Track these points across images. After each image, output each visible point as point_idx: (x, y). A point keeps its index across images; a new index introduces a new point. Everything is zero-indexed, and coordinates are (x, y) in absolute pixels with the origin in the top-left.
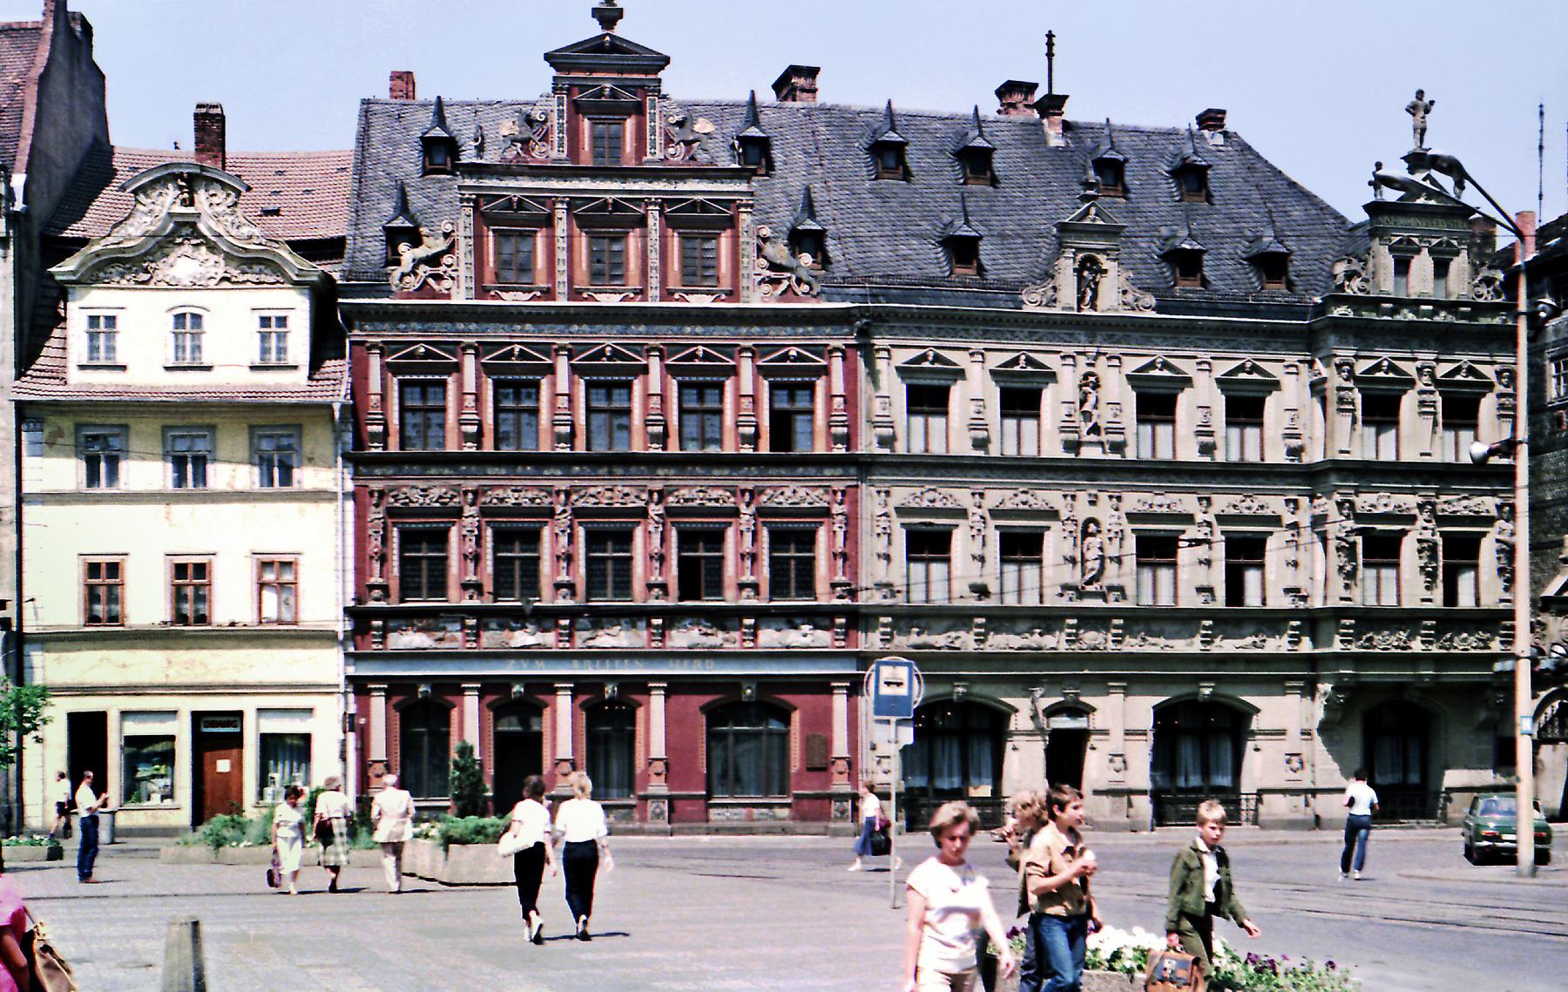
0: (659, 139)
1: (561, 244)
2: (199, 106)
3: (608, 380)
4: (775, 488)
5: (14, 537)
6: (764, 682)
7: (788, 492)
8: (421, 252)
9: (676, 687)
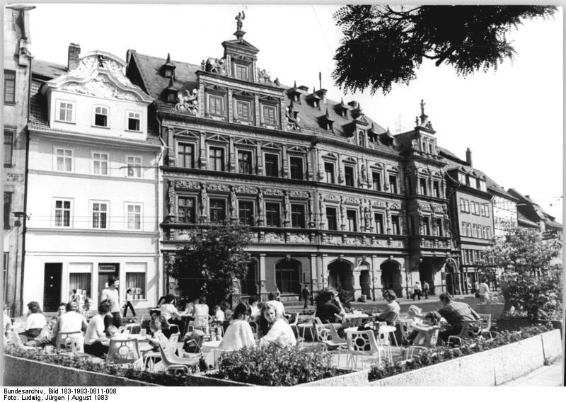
0: (257, 76)
2: (72, 44)
5: (24, 187)
6: (293, 254)
9: (269, 255)
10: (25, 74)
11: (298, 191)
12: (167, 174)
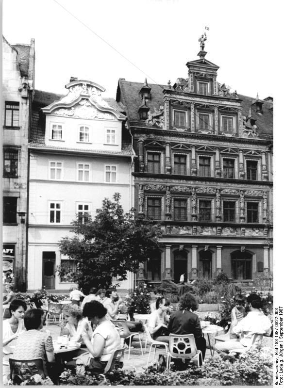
0: (217, 90)
1: (192, 116)
2: (72, 78)
3: (205, 156)
4: (249, 190)
5: (26, 193)
6: (247, 246)
7: (252, 192)
8: (155, 115)
9: (224, 247)
10: (26, 103)
11: (253, 191)
12: (137, 178)
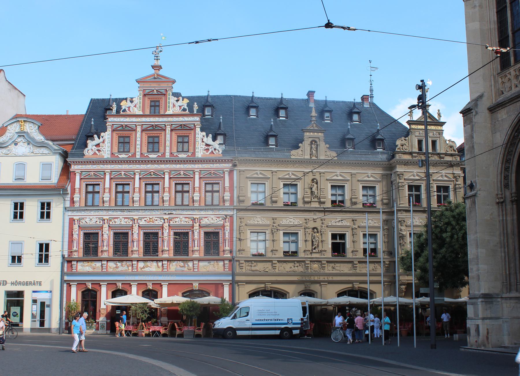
0: (171, 106)
1: (139, 139)
